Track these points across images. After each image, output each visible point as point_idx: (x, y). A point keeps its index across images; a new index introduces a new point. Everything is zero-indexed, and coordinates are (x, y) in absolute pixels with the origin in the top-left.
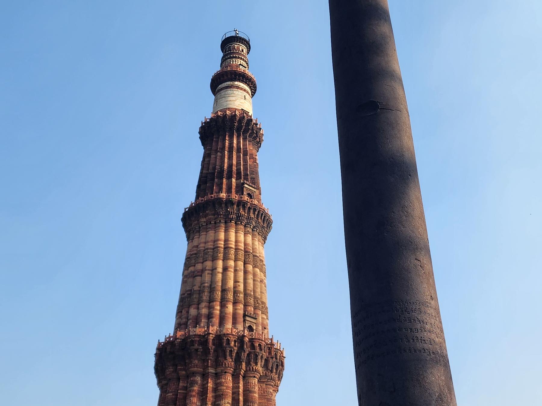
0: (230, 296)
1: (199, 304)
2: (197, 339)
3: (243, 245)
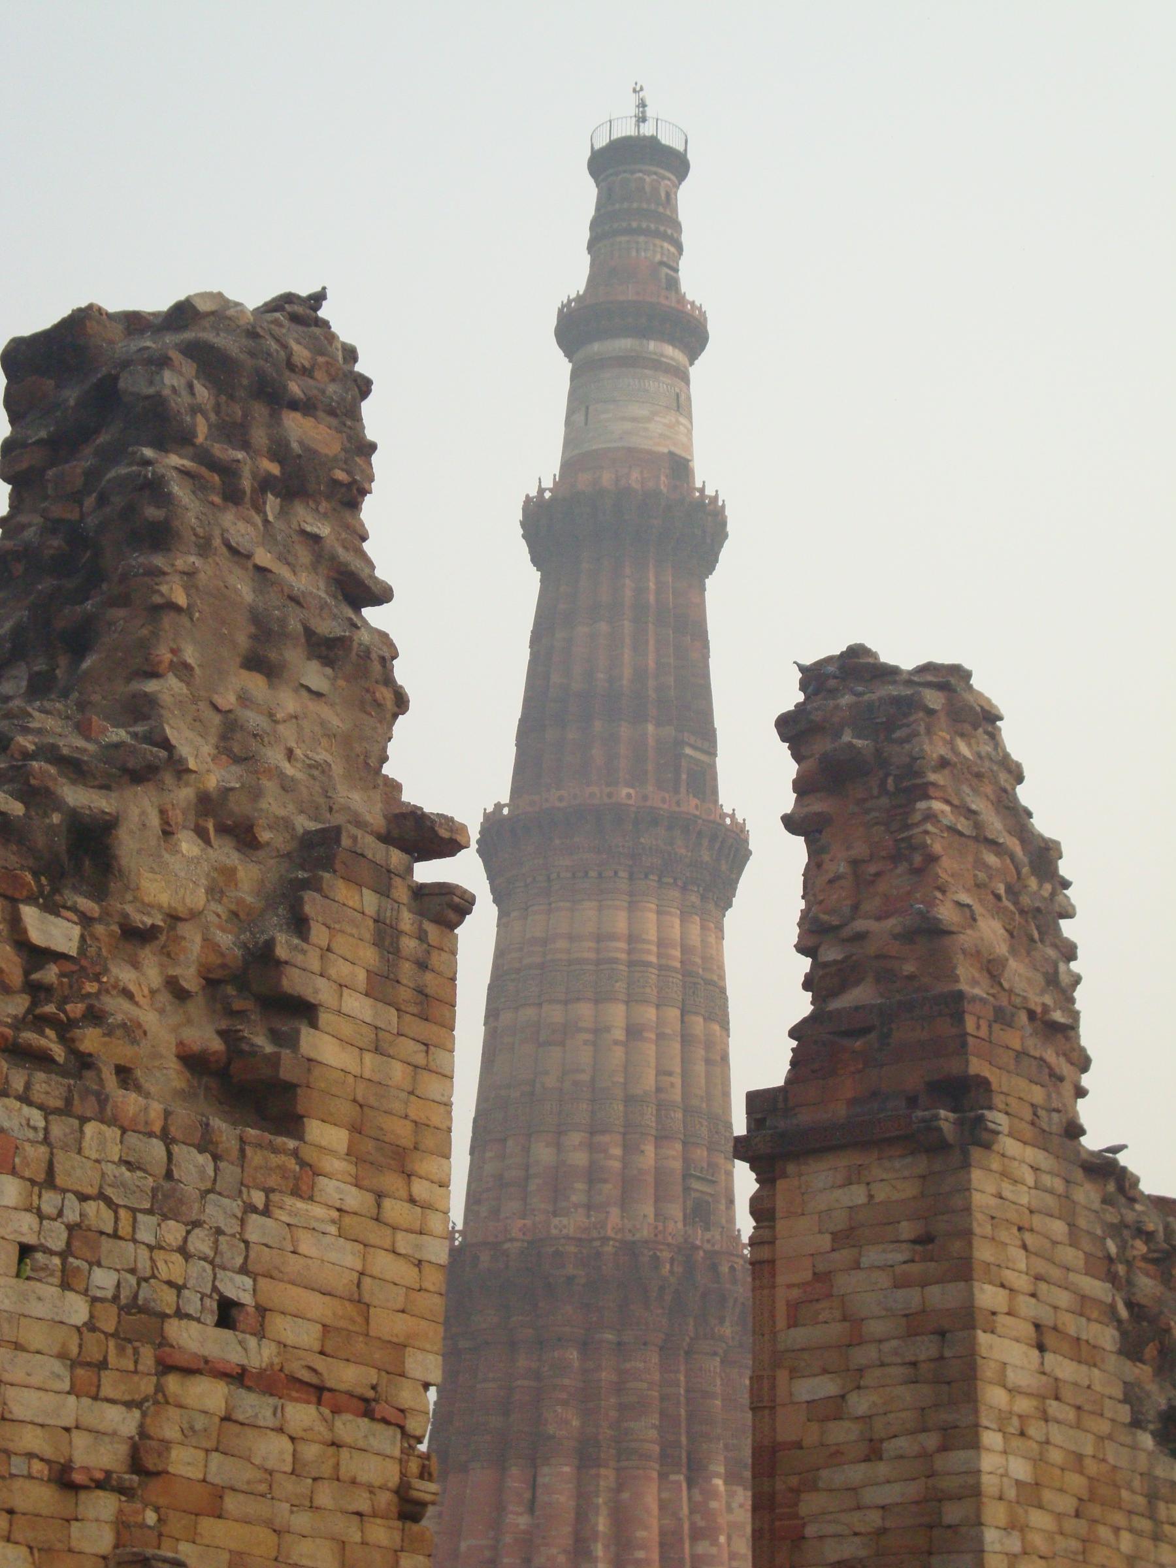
0: (649, 1117)
1: (560, 1133)
2: (573, 1249)
3: (677, 953)
